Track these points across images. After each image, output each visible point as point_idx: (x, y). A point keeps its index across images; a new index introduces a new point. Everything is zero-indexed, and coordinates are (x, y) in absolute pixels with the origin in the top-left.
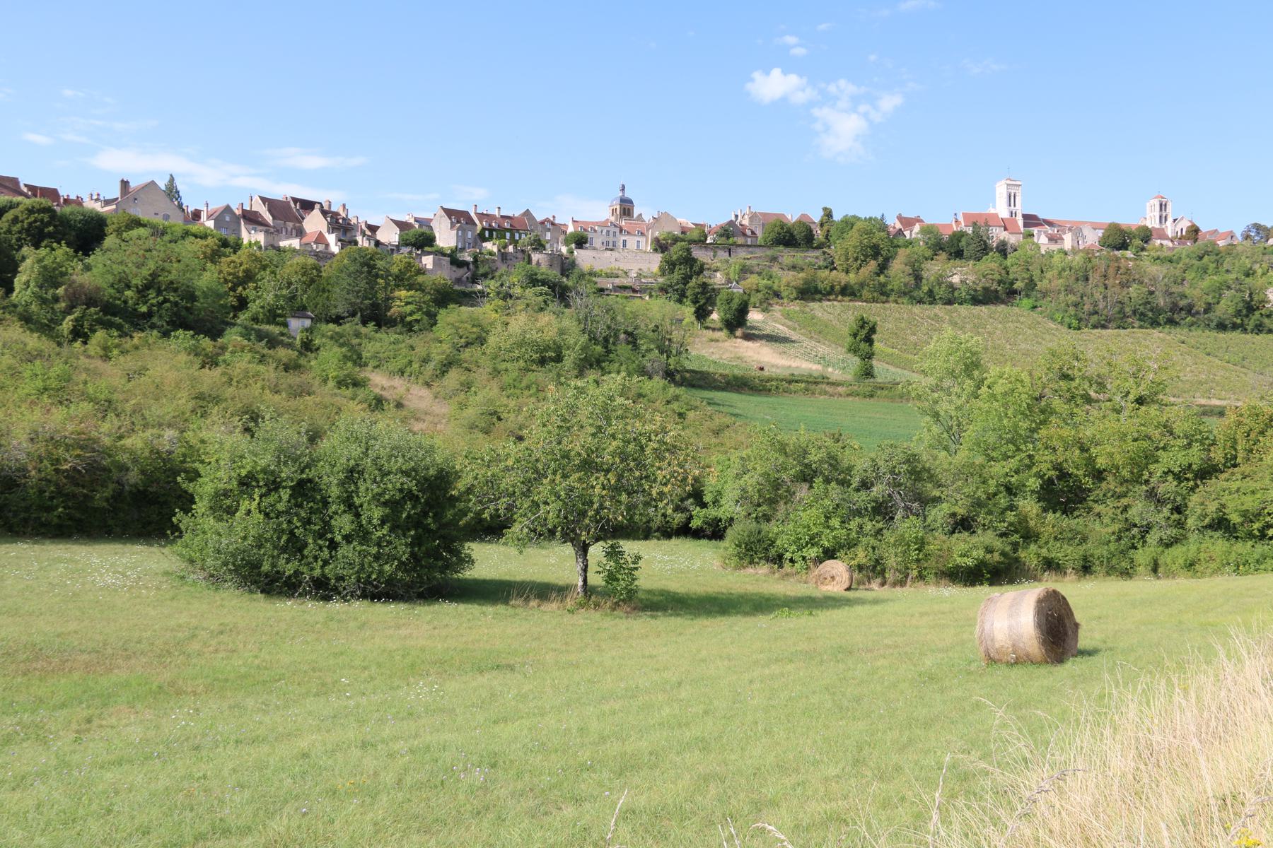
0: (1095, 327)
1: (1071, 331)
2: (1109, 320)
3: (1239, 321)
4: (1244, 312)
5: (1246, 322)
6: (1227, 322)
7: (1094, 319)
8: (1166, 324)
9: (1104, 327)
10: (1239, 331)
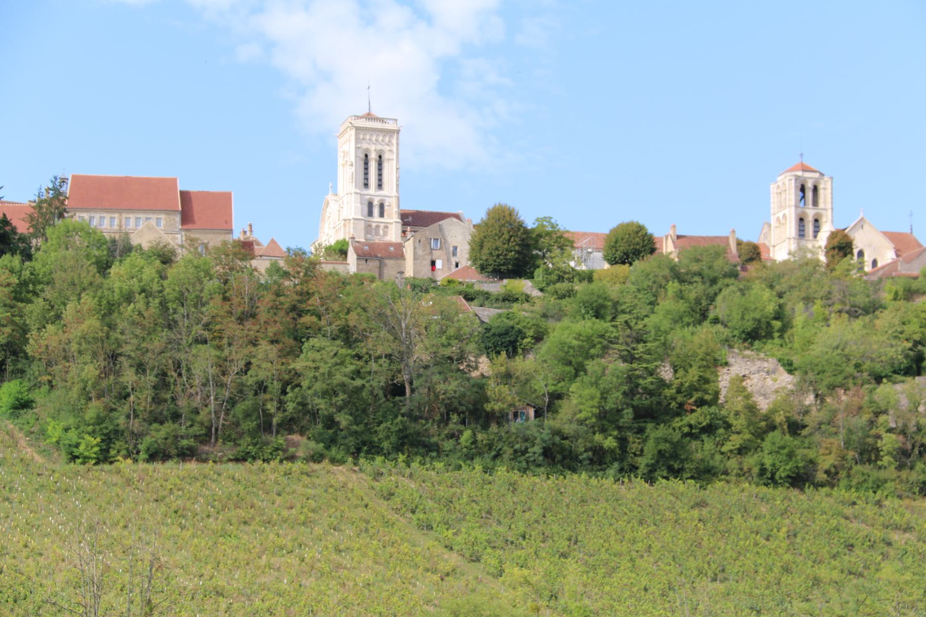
0: (157, 455)
1: (77, 466)
2: (206, 437)
3: (610, 443)
4: (628, 414)
5: (634, 447)
6: (580, 446)
7: (158, 434)
8: (398, 448)
9: (186, 455)
10: (611, 472)
